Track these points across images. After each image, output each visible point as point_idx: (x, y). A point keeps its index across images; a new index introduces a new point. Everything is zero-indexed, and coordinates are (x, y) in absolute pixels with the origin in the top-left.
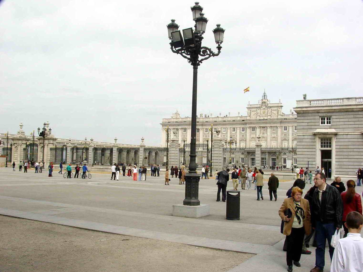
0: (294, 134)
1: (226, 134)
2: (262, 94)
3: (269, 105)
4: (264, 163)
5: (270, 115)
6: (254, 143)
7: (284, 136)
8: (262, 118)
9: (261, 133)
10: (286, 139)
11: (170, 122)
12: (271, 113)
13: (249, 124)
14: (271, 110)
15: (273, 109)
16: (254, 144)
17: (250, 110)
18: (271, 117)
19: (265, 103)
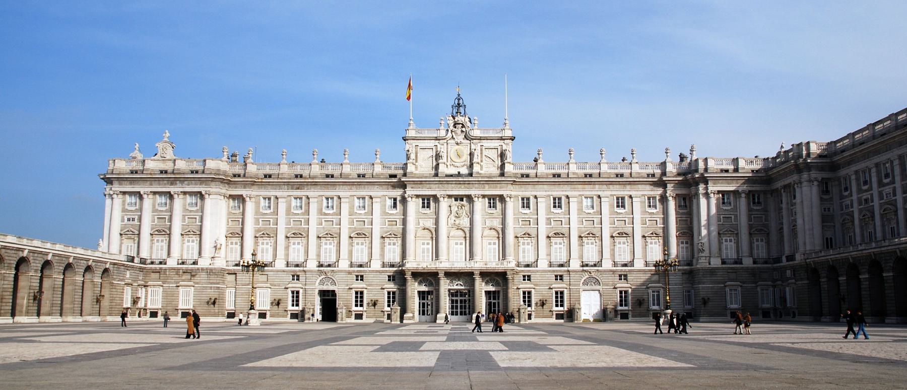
0: (552, 221)
1: (337, 215)
2: (452, 101)
3: (476, 133)
4: (465, 306)
5: (478, 163)
6: (428, 244)
7: (523, 227)
8: (454, 171)
9: (451, 213)
10: (529, 235)
11: (139, 172)
12: (482, 157)
13: (412, 188)
14: (479, 148)
15: (486, 144)
16: (428, 249)
17: (414, 145)
18: (481, 169)
19: (462, 127)
